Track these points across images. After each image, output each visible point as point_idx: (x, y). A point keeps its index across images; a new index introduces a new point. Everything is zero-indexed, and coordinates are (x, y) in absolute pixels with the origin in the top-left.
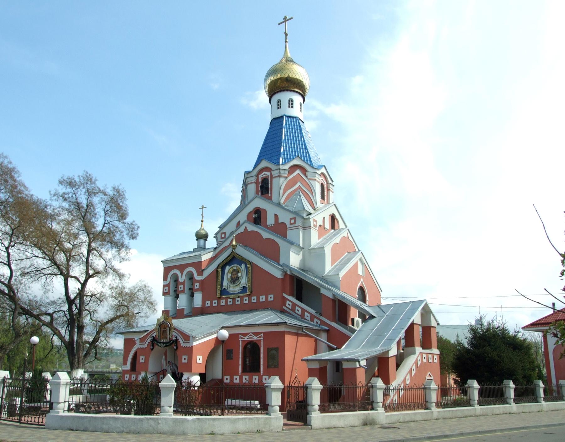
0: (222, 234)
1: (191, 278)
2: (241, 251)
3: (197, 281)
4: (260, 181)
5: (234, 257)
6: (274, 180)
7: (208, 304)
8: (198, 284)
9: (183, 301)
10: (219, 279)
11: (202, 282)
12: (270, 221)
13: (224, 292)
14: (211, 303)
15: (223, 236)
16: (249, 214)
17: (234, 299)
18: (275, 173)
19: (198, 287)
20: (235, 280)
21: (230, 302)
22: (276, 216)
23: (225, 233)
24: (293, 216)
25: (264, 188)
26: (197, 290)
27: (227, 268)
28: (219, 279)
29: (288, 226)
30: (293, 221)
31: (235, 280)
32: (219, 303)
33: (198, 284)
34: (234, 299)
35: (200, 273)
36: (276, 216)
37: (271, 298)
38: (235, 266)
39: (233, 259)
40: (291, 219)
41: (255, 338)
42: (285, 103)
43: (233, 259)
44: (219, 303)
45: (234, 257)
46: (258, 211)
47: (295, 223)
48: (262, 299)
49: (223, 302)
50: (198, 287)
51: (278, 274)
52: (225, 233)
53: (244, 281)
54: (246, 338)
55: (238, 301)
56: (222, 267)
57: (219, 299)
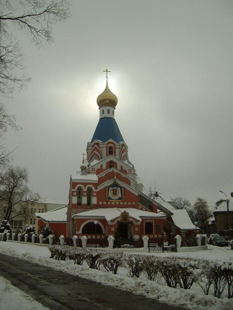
1: (90, 190)
2: (119, 182)
3: (95, 192)
5: (115, 184)
6: (116, 149)
7: (101, 203)
9: (84, 200)
10: (107, 193)
11: (97, 193)
12: (119, 168)
13: (110, 198)
14: (103, 203)
18: (117, 146)
20: (115, 193)
21: (113, 203)
22: (122, 167)
23: (94, 169)
25: (111, 152)
26: (94, 196)
27: (111, 188)
28: (107, 193)
29: (128, 172)
31: (115, 193)
32: (107, 203)
35: (96, 188)
36: (122, 167)
37: (134, 203)
38: (115, 188)
39: (115, 185)
41: (151, 221)
42: (111, 112)
43: (115, 185)
44: (107, 203)
45: (115, 184)
46: (112, 162)
48: (130, 203)
49: (109, 203)
51: (137, 194)
53: (120, 195)
54: (147, 221)
56: (109, 187)
57: (107, 202)
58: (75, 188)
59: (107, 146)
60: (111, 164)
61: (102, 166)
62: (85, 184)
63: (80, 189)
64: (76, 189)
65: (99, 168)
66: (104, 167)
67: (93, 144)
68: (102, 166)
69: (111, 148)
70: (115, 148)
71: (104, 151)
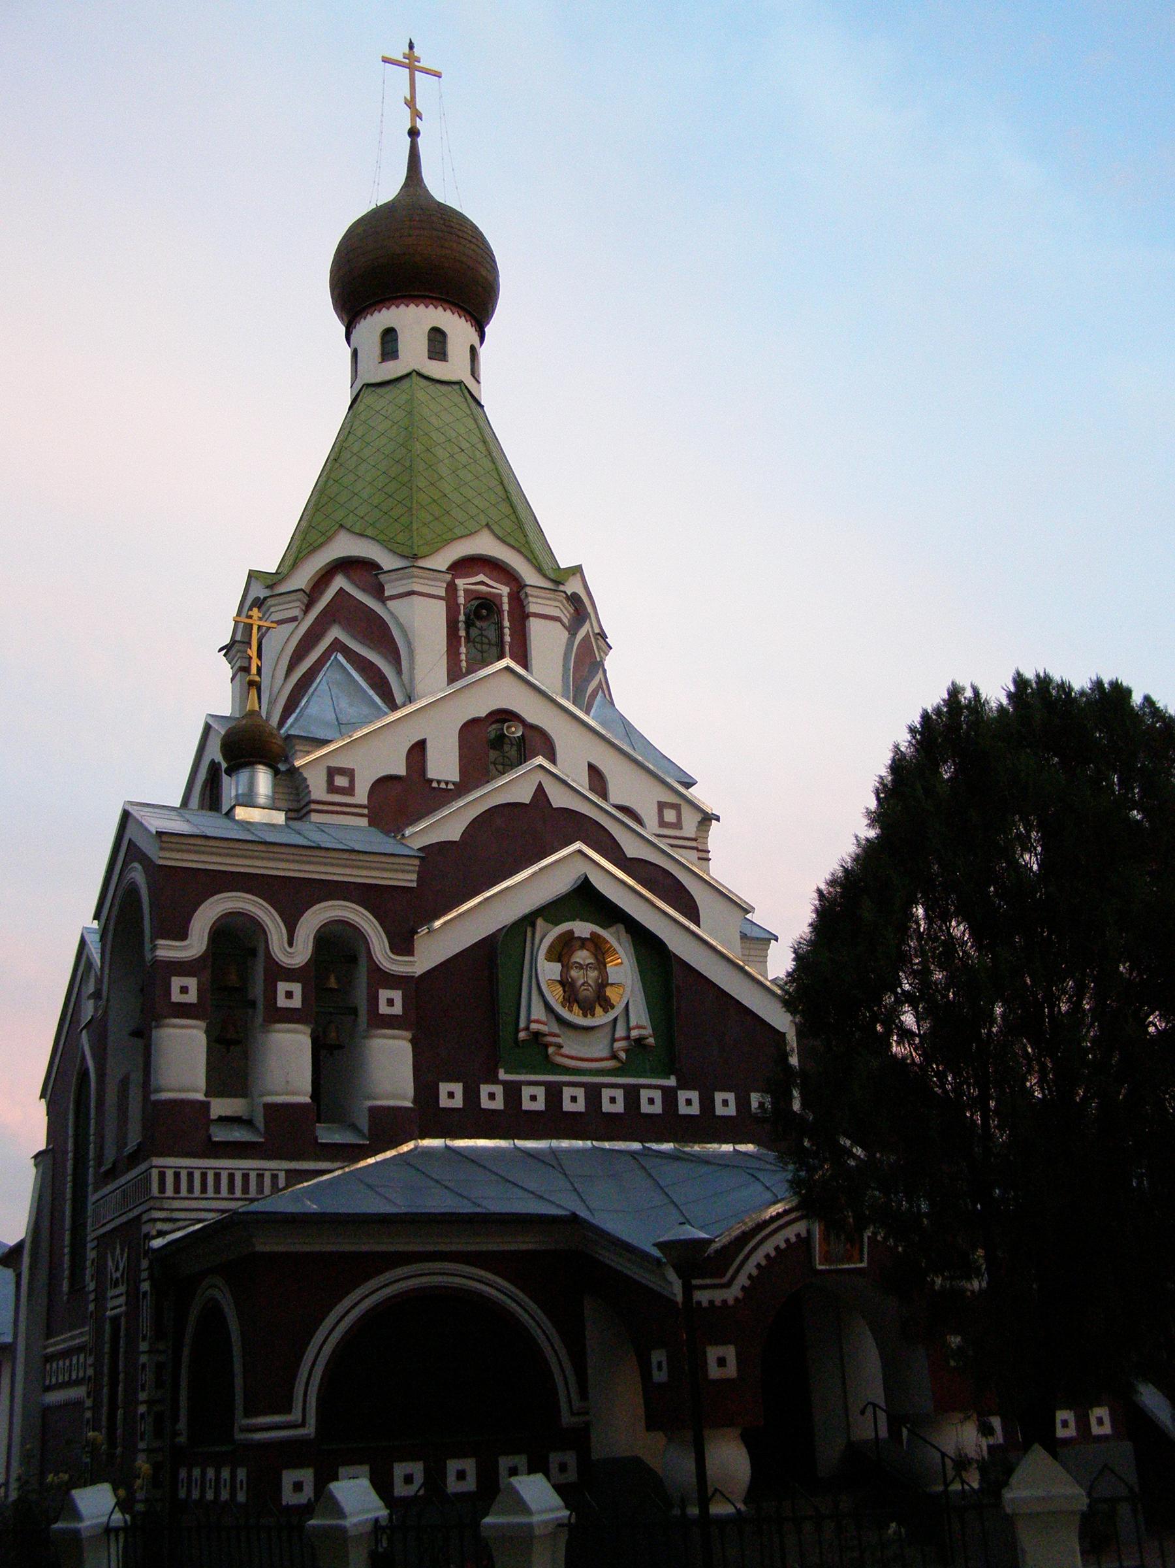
0: (332, 772)
4: (461, 600)
8: (397, 995)
11: (416, 989)
15: (340, 781)
16: (470, 727)
17: (593, 1094)
19: (397, 1009)
24: (671, 798)
30: (670, 816)
33: (397, 995)
34: (593, 1094)
35: (403, 944)
36: (596, 776)
40: (662, 806)
47: (678, 825)
50: (397, 1009)
52: (350, 773)
55: (613, 1103)
58: (182, 935)
59: (451, 588)
60: (497, 741)
61: (418, 750)
62: (292, 896)
63: (235, 943)
64: (195, 944)
65: (399, 768)
66: (444, 765)
67: (302, 579)
68: (418, 750)
69: (484, 607)
70: (521, 616)
71: (423, 622)
